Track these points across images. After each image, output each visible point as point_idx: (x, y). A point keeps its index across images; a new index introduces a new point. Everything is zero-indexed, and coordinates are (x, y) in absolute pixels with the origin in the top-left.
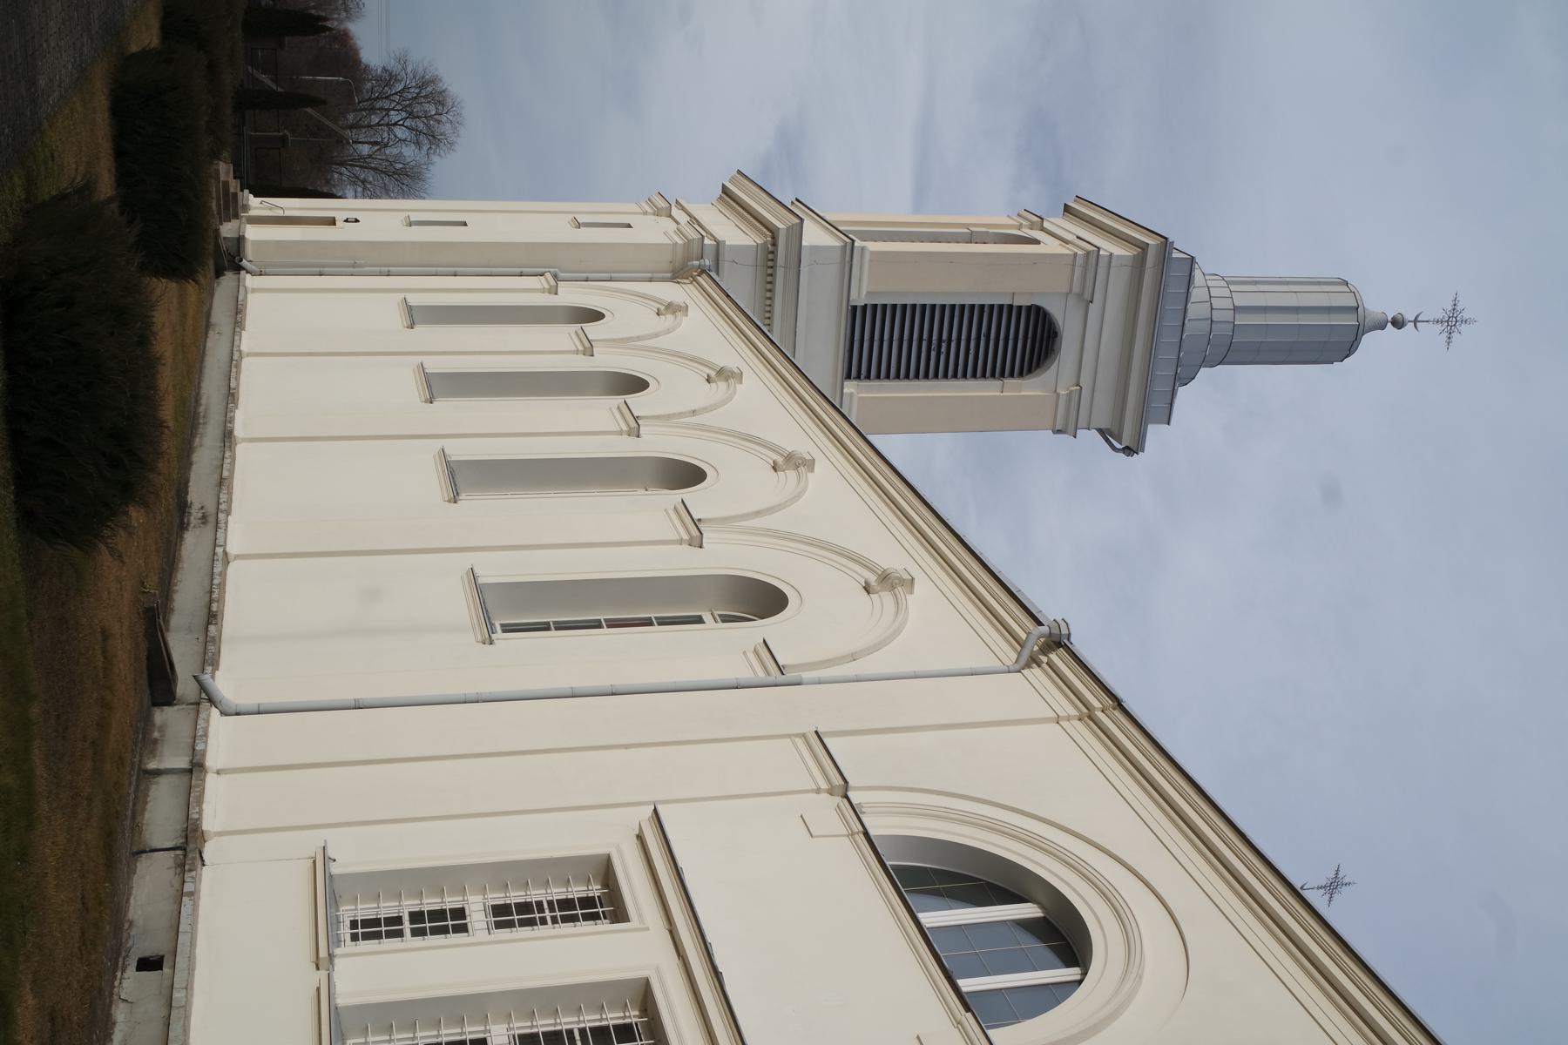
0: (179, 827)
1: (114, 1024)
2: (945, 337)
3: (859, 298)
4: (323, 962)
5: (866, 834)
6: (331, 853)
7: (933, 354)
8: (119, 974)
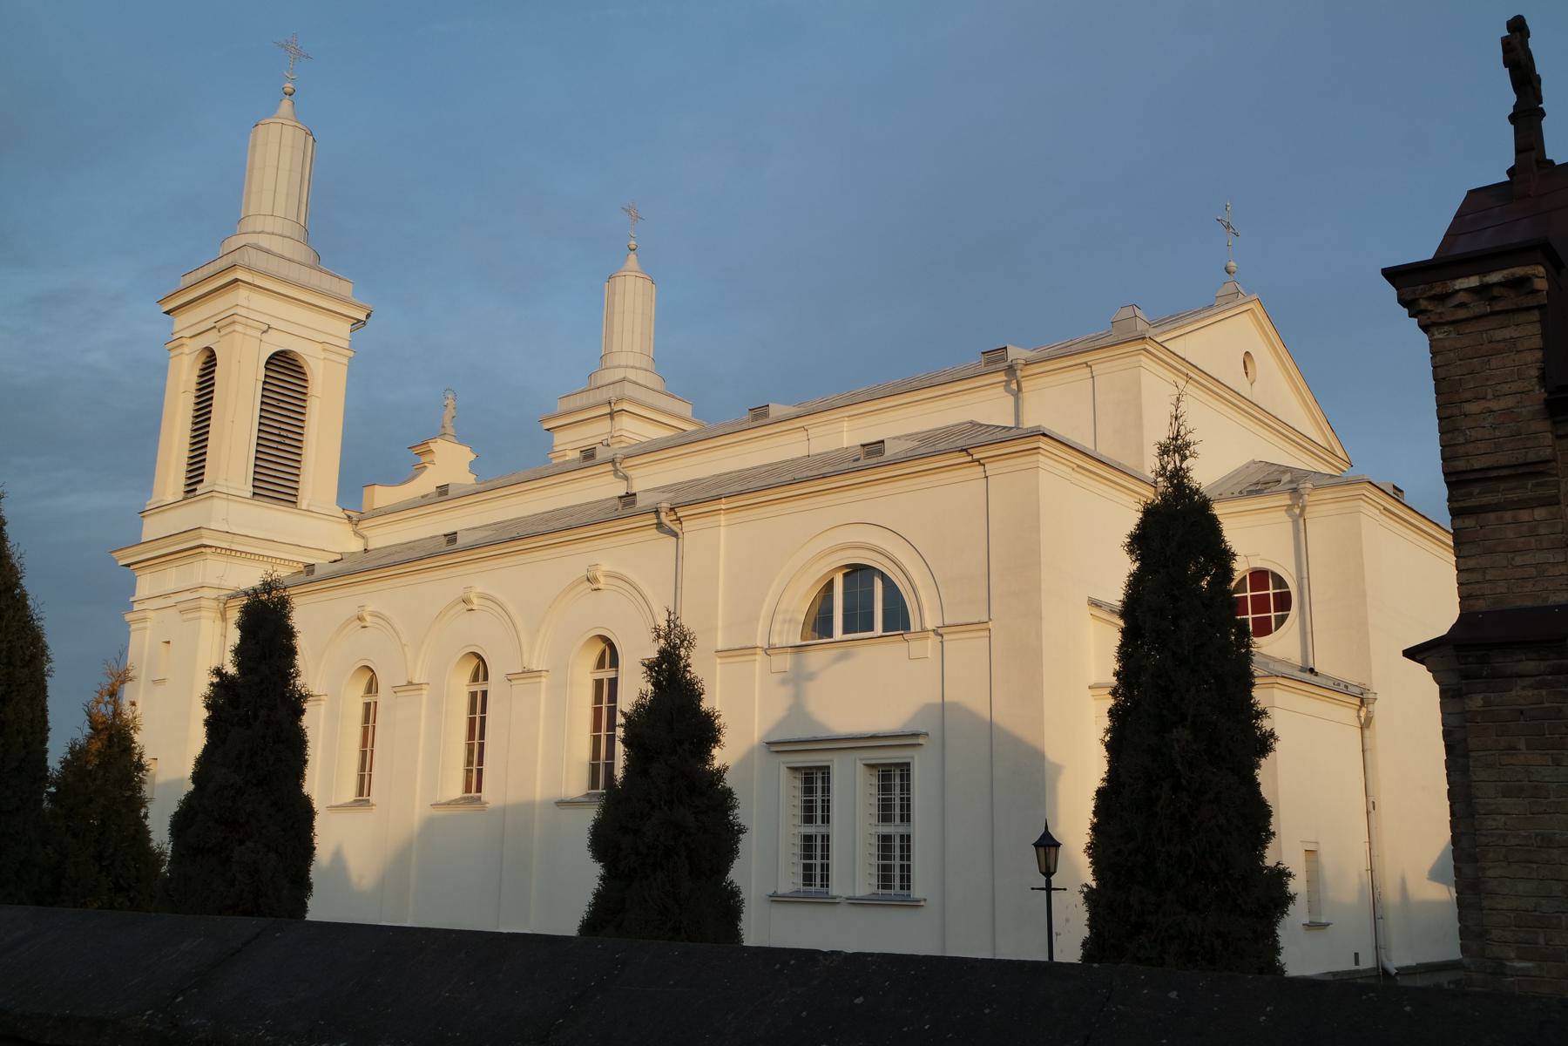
2: (276, 432)
3: (248, 490)
6: (771, 893)
7: (288, 441)
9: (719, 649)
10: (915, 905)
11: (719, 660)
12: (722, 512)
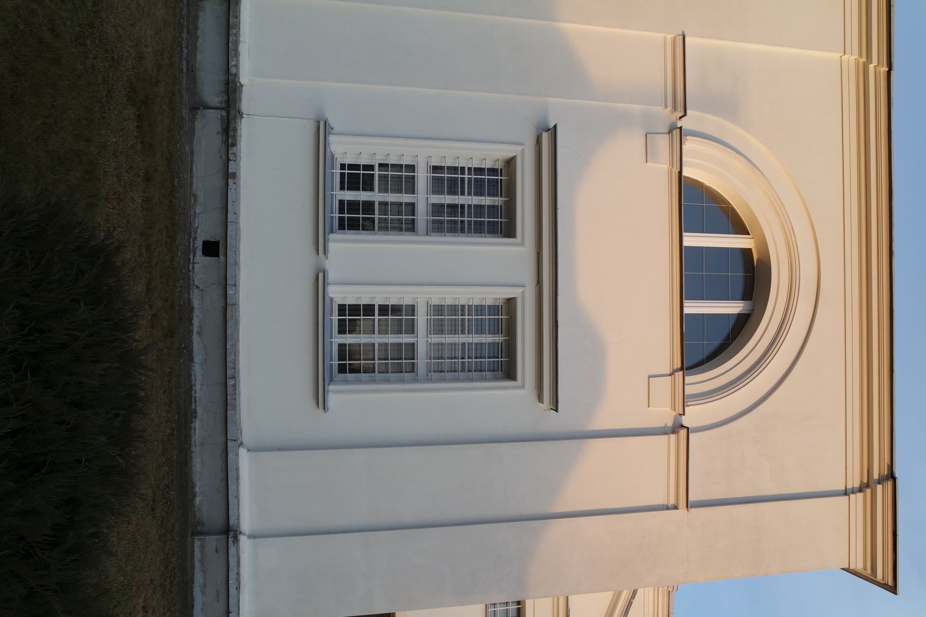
0: (222, 78)
1: (193, 308)
4: (319, 246)
5: (680, 173)
8: (191, 256)
9: (687, 39)
10: (320, 399)
11: (670, 37)
12: (864, 59)
